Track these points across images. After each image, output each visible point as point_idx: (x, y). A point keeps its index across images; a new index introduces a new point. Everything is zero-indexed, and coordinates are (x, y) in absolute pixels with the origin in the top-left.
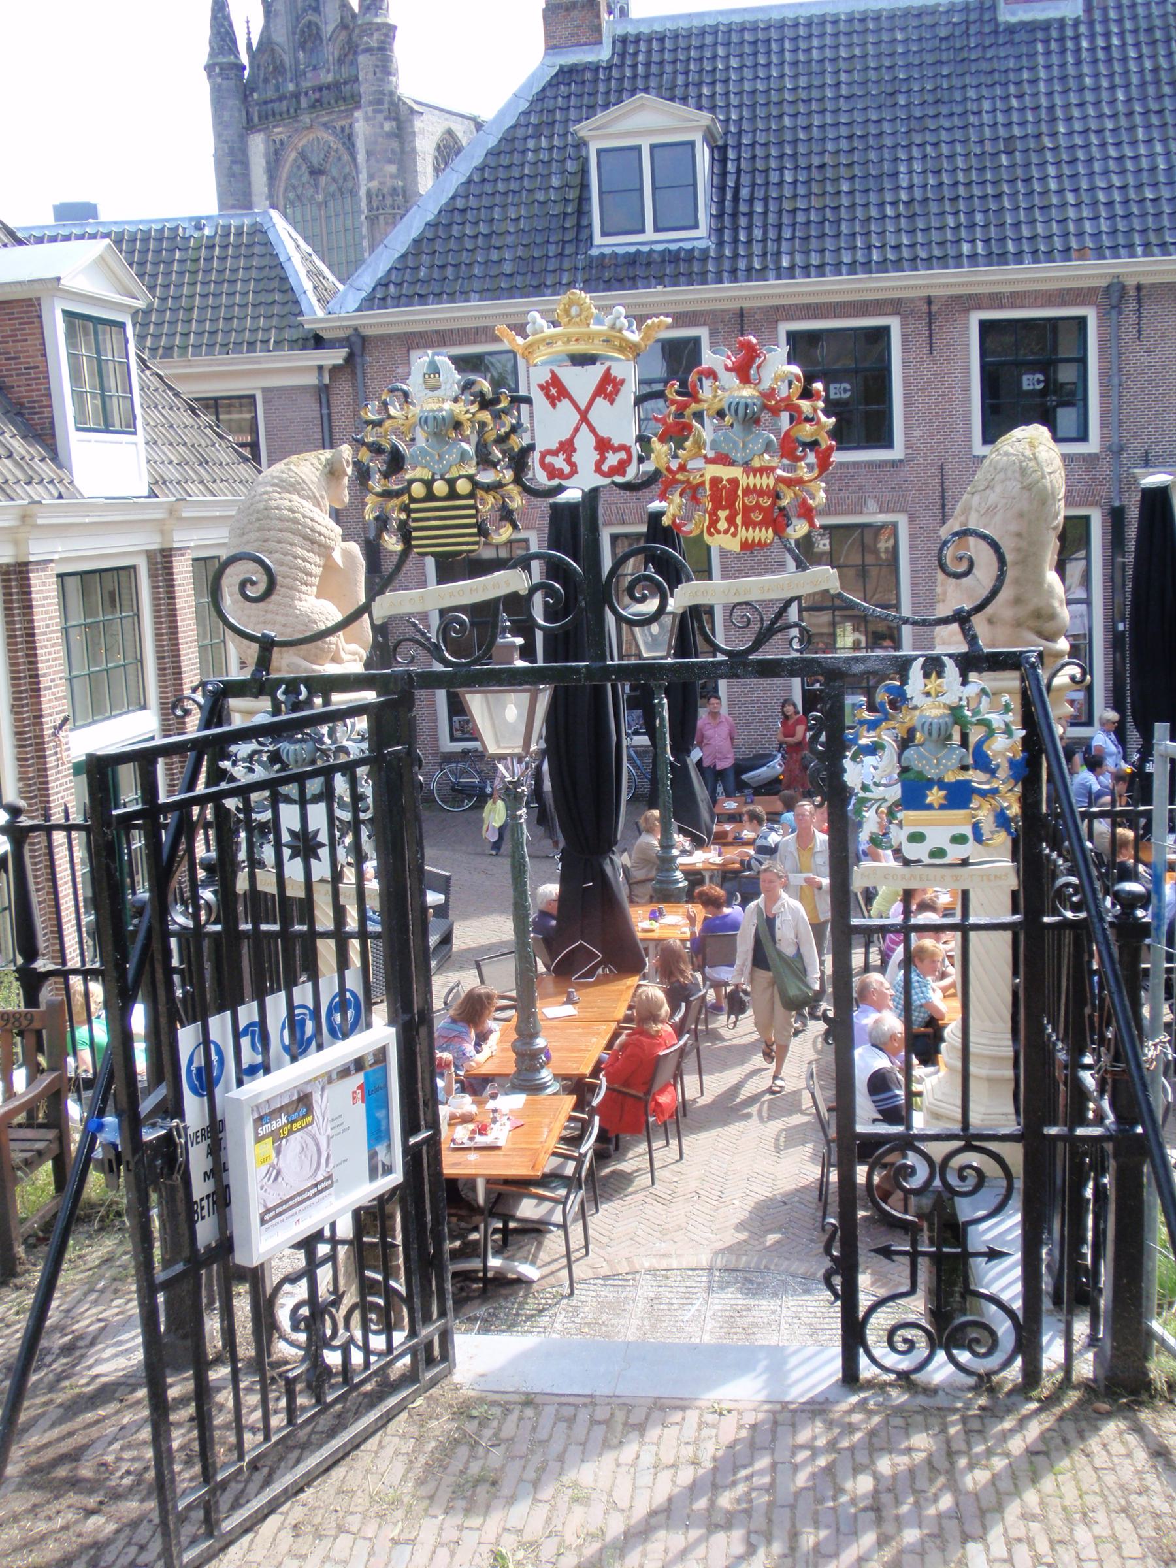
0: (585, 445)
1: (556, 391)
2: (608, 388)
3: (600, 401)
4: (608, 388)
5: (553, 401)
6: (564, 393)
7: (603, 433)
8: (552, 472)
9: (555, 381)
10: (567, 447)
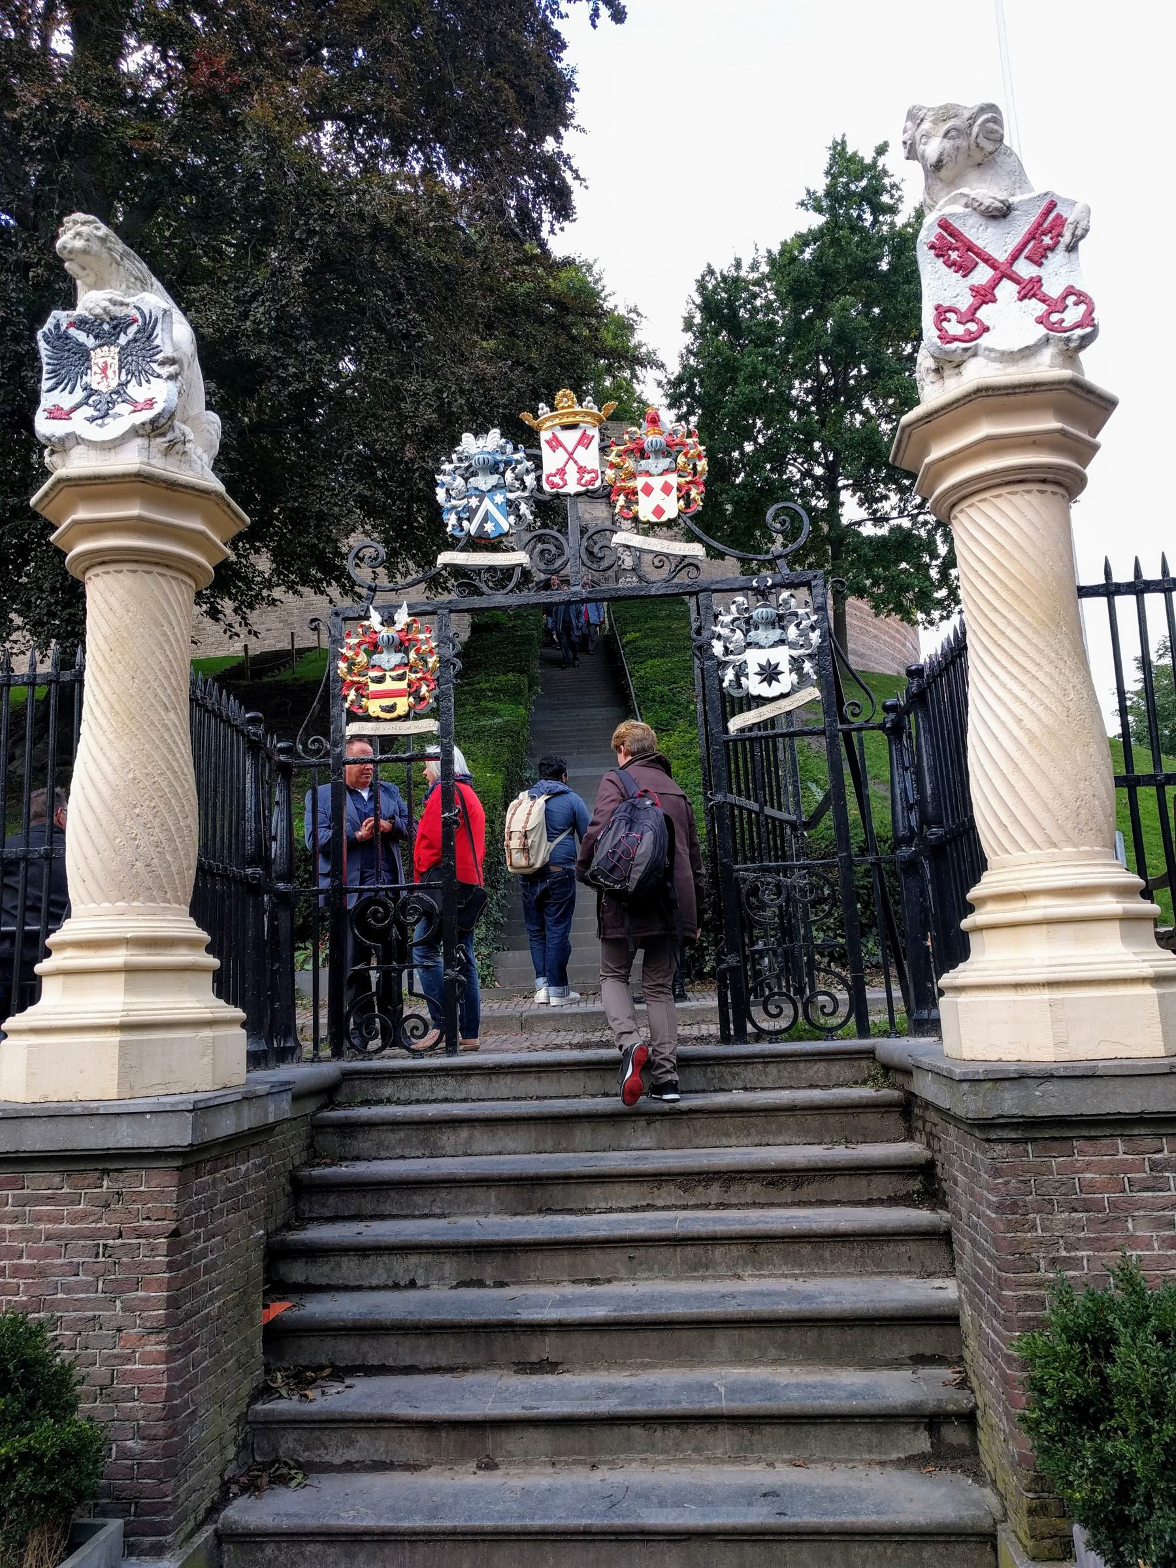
0: (571, 469)
1: (555, 443)
2: (584, 441)
4: (584, 441)
5: (554, 449)
6: (562, 445)
7: (582, 464)
8: (553, 485)
9: (555, 437)
10: (562, 472)
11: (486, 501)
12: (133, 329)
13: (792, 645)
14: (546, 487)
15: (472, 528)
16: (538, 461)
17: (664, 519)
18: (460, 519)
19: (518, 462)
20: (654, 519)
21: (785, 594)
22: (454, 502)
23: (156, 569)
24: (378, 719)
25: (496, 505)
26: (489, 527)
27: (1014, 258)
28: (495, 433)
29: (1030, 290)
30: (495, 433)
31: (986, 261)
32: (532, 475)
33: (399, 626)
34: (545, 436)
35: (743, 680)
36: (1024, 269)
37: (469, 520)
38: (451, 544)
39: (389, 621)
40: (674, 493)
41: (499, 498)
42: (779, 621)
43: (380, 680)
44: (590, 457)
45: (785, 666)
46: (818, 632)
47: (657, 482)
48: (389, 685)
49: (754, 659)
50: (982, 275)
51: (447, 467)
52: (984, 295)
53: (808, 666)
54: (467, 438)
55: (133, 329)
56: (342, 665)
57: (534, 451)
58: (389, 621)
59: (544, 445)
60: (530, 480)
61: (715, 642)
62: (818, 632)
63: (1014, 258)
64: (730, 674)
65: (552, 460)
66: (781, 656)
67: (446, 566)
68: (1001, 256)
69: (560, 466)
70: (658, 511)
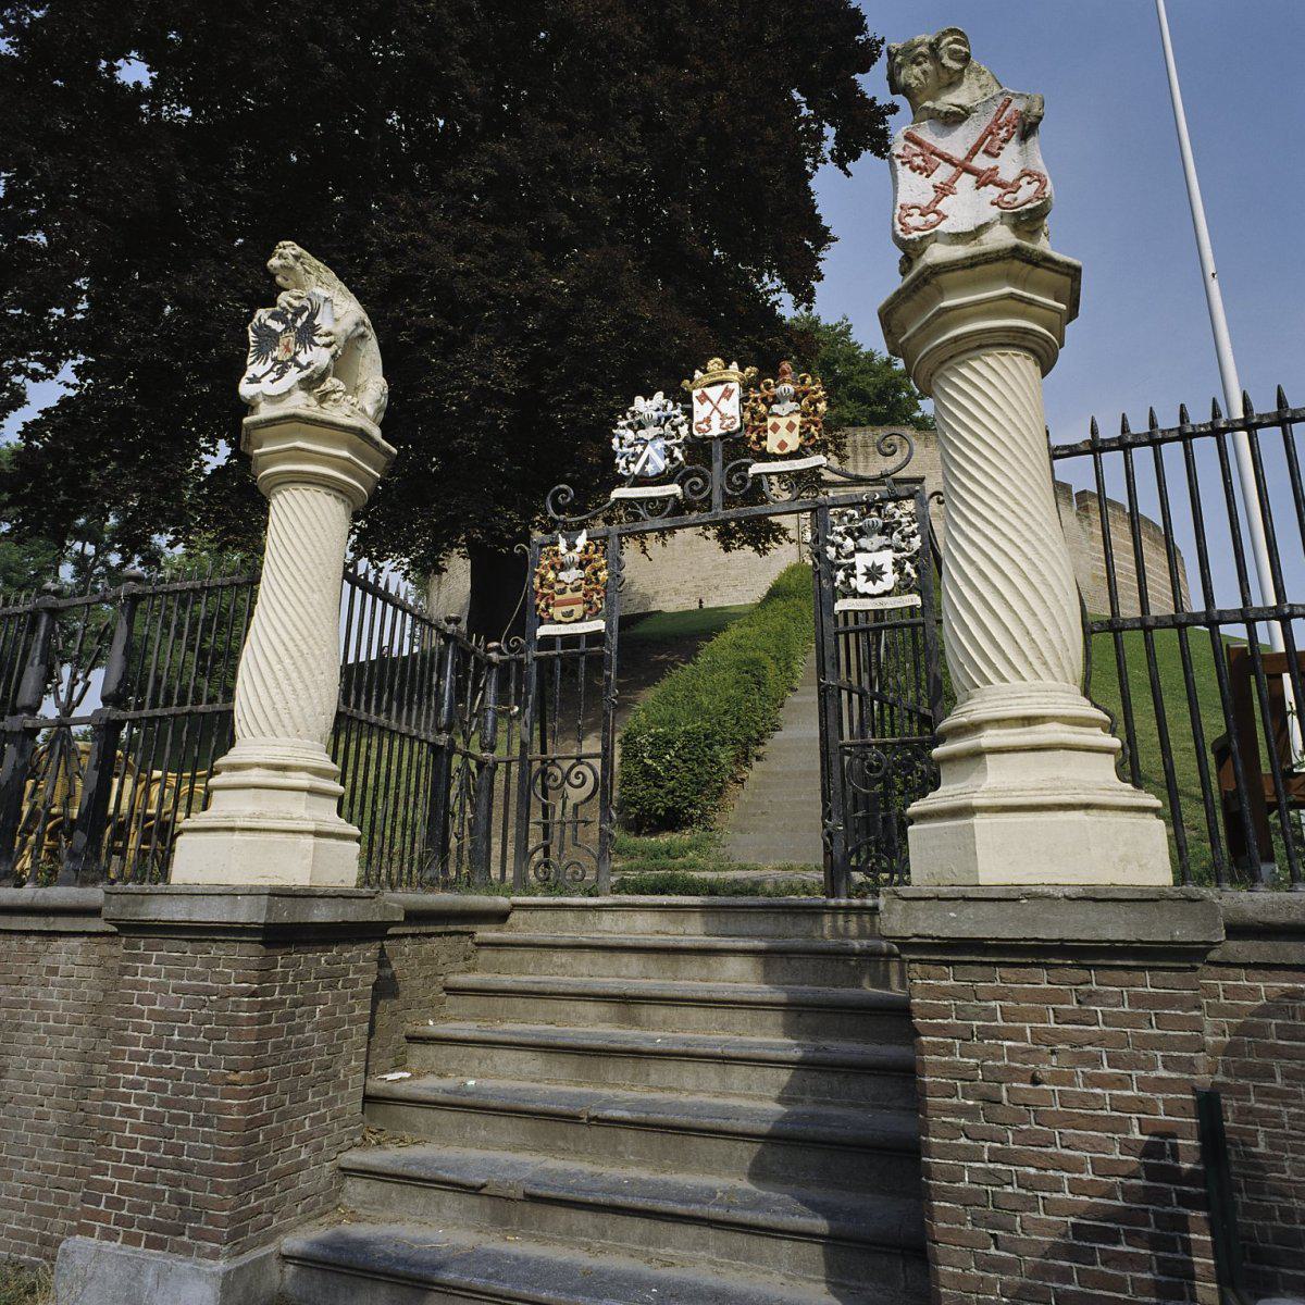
0: (716, 417)
1: (704, 398)
2: (727, 394)
3: (723, 400)
5: (702, 402)
7: (723, 412)
10: (708, 420)
11: (649, 447)
12: (306, 314)
13: (899, 550)
14: (695, 433)
15: (636, 469)
16: (689, 413)
17: (787, 451)
18: (628, 463)
19: (676, 417)
20: (778, 451)
21: (891, 505)
22: (625, 450)
23: (341, 496)
24: (560, 622)
25: (656, 450)
26: (650, 469)
27: (973, 152)
28: (659, 396)
29: (984, 179)
30: (659, 396)
31: (946, 160)
32: (686, 426)
33: (579, 549)
34: (696, 393)
35: (852, 580)
36: (981, 162)
37: (635, 463)
38: (620, 481)
39: (571, 547)
40: (797, 430)
41: (660, 444)
42: (886, 530)
43: (562, 592)
44: (732, 407)
45: (888, 568)
46: (918, 537)
47: (783, 422)
48: (569, 594)
49: (862, 561)
50: (944, 172)
51: (621, 423)
52: (943, 190)
53: (908, 567)
54: (639, 400)
55: (306, 314)
56: (537, 581)
57: (688, 406)
58: (571, 547)
59: (694, 400)
60: (684, 431)
61: (829, 548)
62: (918, 537)
63: (973, 152)
64: (841, 575)
65: (701, 411)
66: (886, 559)
67: (617, 499)
68: (959, 154)
69: (706, 415)
70: (783, 445)
